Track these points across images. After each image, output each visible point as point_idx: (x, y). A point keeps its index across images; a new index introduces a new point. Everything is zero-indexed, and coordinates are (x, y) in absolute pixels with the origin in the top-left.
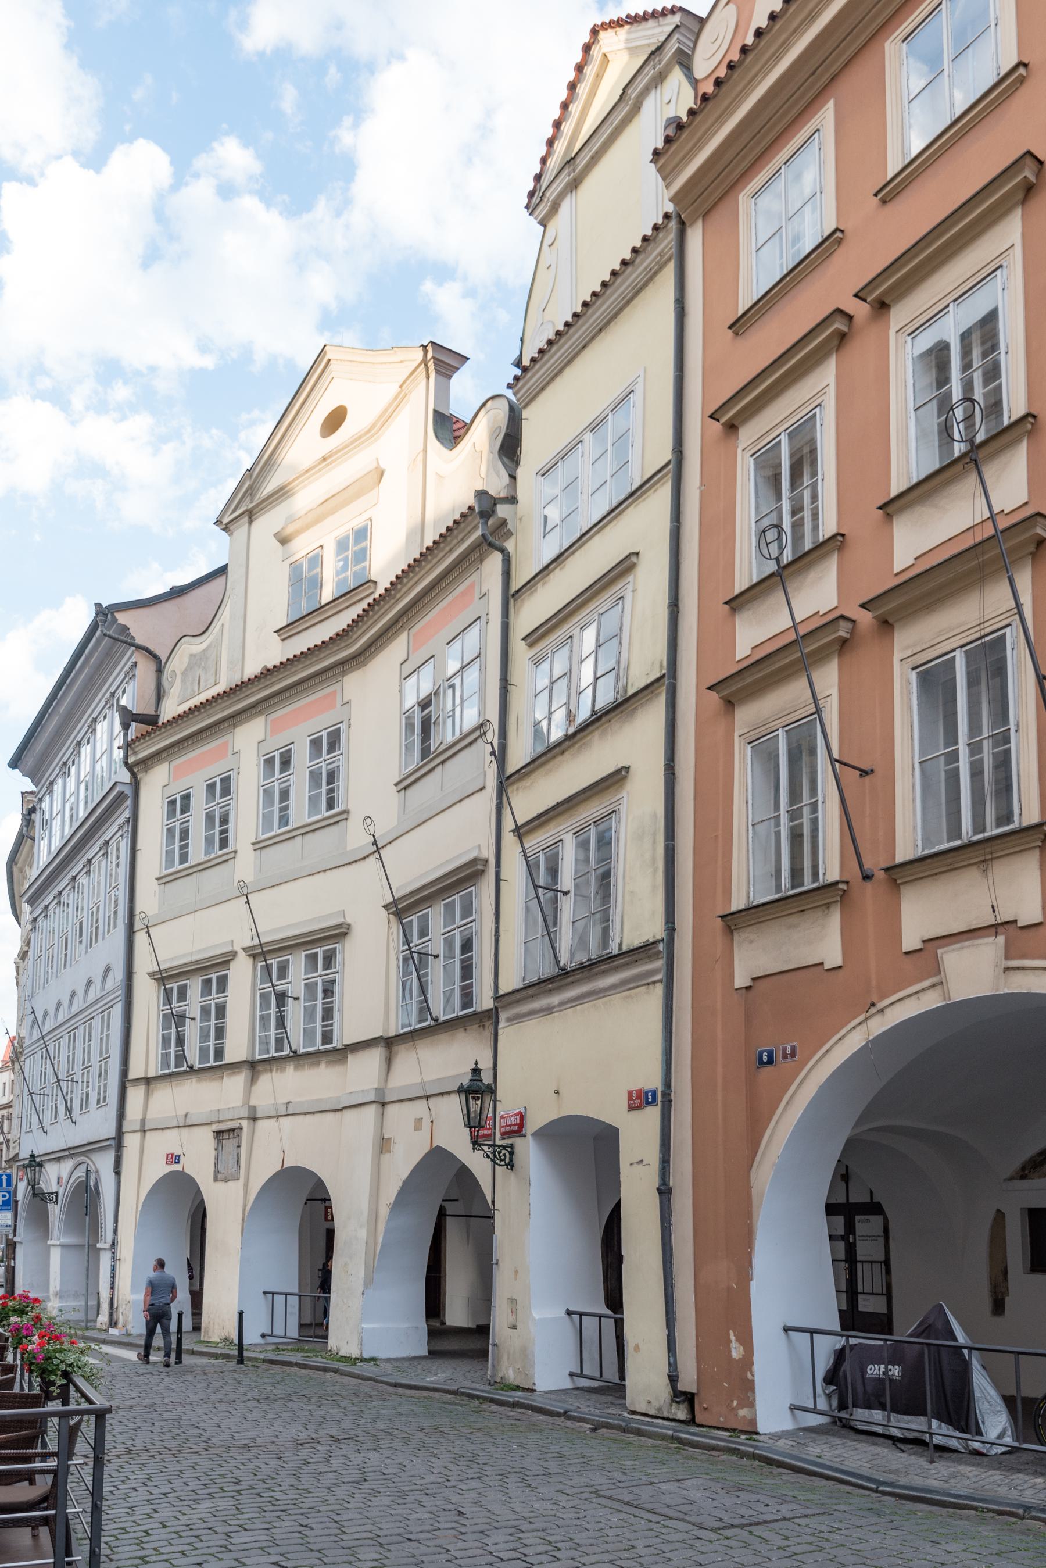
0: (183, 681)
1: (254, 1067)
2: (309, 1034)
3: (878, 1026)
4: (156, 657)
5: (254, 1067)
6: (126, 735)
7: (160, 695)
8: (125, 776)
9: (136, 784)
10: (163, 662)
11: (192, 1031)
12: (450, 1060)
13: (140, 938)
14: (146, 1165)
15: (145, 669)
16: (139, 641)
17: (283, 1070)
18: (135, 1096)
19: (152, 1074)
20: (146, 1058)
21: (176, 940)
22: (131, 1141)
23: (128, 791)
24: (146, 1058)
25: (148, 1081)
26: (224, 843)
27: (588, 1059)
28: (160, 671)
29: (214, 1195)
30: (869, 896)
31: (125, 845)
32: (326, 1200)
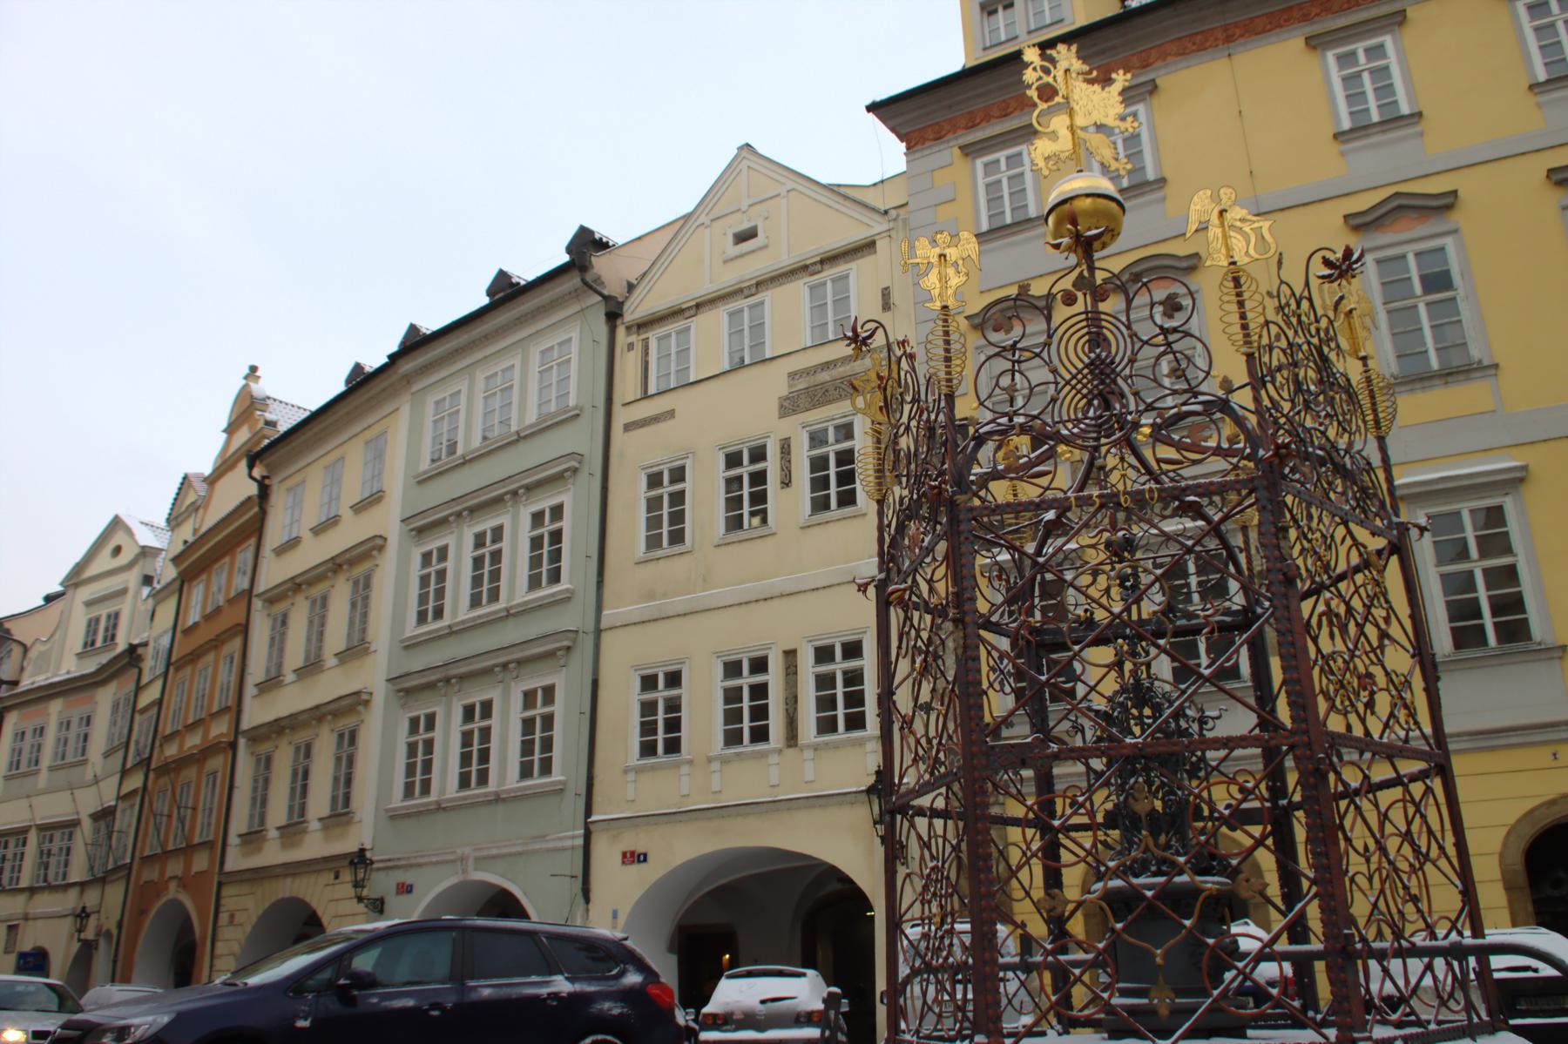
1: (32, 891)
4: (24, 646)
5: (32, 891)
26: (37, 763)
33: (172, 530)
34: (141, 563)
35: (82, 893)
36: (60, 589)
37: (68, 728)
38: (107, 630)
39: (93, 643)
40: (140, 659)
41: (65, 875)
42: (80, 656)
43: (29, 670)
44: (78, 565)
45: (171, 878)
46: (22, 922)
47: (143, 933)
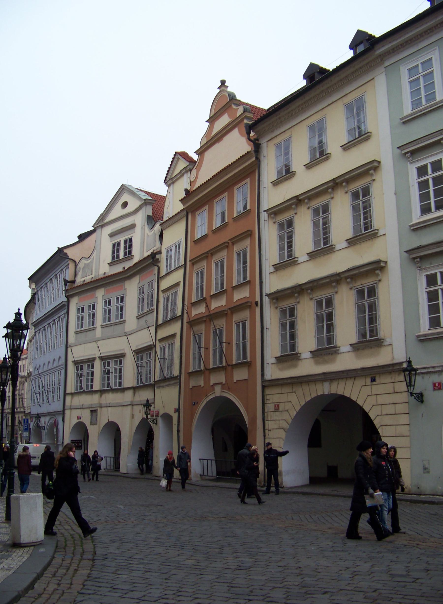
0: (83, 271)
1: (102, 392)
2: (115, 383)
3: (208, 399)
4: (75, 262)
6: (66, 288)
7: (76, 275)
8: (66, 299)
9: (68, 302)
10: (77, 263)
11: (84, 379)
12: (145, 395)
13: (69, 350)
14: (71, 419)
15: (72, 266)
16: (70, 257)
17: (109, 393)
18: (68, 398)
19: (73, 392)
20: (71, 388)
21: (79, 352)
22: (67, 412)
23: (66, 304)
24: (71, 388)
25: (72, 394)
26: (93, 324)
27: (167, 399)
28: (76, 266)
29: (90, 429)
30: (207, 372)
31: (65, 320)
32: (120, 430)
33: (169, 186)
34: (144, 209)
35: (134, 393)
36: (93, 228)
37: (110, 304)
38: (125, 248)
39: (118, 256)
40: (158, 261)
41: (120, 384)
42: (110, 264)
43: (80, 274)
44: (102, 214)
45: (214, 384)
46: (98, 408)
47: (197, 416)
